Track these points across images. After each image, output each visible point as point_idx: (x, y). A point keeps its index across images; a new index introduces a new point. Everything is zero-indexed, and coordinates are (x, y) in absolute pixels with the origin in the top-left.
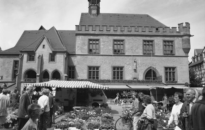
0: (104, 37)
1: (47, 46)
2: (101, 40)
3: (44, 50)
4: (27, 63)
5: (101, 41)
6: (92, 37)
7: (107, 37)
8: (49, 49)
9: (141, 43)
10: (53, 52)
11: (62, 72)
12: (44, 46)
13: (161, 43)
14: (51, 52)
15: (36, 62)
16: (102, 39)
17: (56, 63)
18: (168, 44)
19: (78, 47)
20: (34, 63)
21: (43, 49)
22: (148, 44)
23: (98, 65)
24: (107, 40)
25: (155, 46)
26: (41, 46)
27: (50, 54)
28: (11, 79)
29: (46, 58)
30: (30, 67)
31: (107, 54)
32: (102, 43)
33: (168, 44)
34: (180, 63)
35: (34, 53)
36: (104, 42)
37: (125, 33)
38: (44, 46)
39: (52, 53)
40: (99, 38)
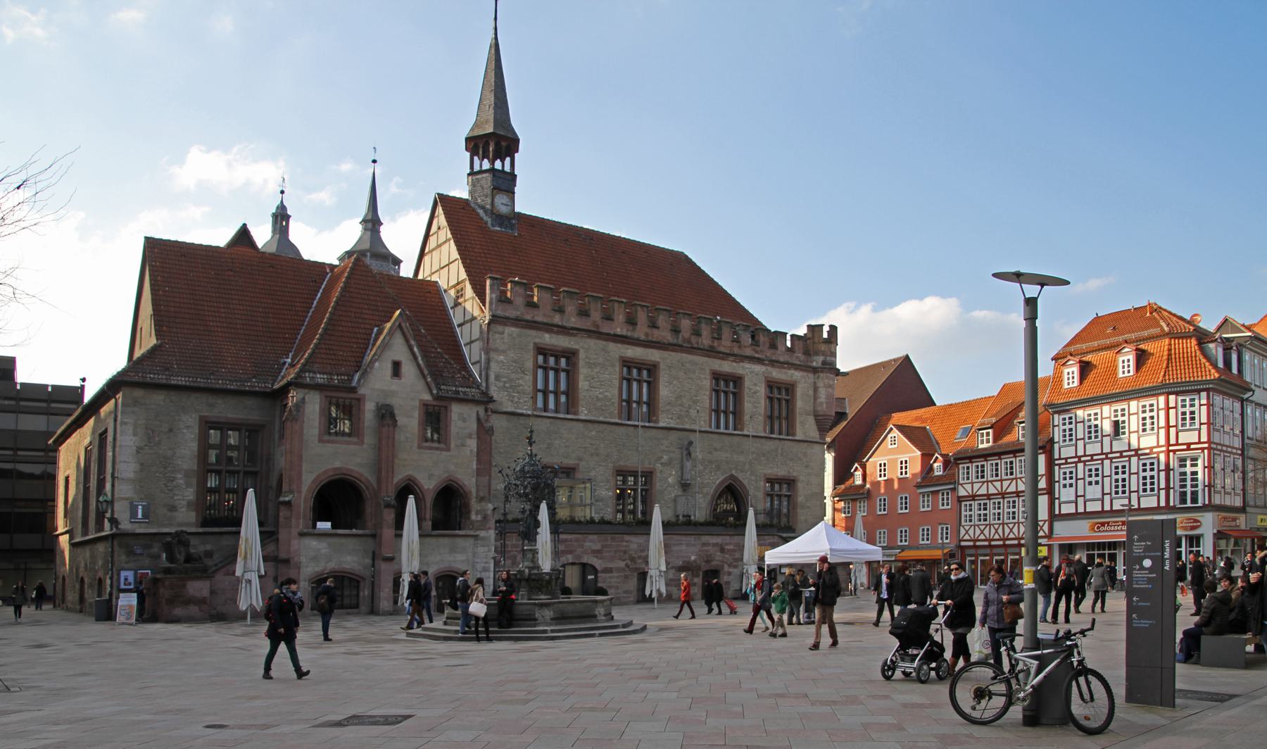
0: (594, 343)
1: (408, 369)
2: (582, 355)
3: (395, 385)
4: (321, 441)
5: (581, 363)
6: (548, 339)
7: (601, 343)
8: (421, 385)
9: (707, 383)
10: (437, 398)
11: (474, 491)
12: (397, 366)
13: (762, 390)
14: (427, 397)
15: (362, 443)
16: (587, 348)
17: (448, 450)
18: (781, 395)
19: (497, 378)
20: (355, 444)
21: (396, 381)
22: (729, 386)
23: (570, 462)
24: (601, 360)
25: (746, 399)
26: (382, 370)
27: (425, 405)
28: (193, 520)
29: (410, 422)
30: (337, 464)
31: (601, 419)
32: (583, 371)
33: (781, 395)
34: (807, 467)
35: (352, 395)
36: (590, 365)
37: (665, 335)
38: (397, 366)
39: (435, 403)
40: (576, 347)
